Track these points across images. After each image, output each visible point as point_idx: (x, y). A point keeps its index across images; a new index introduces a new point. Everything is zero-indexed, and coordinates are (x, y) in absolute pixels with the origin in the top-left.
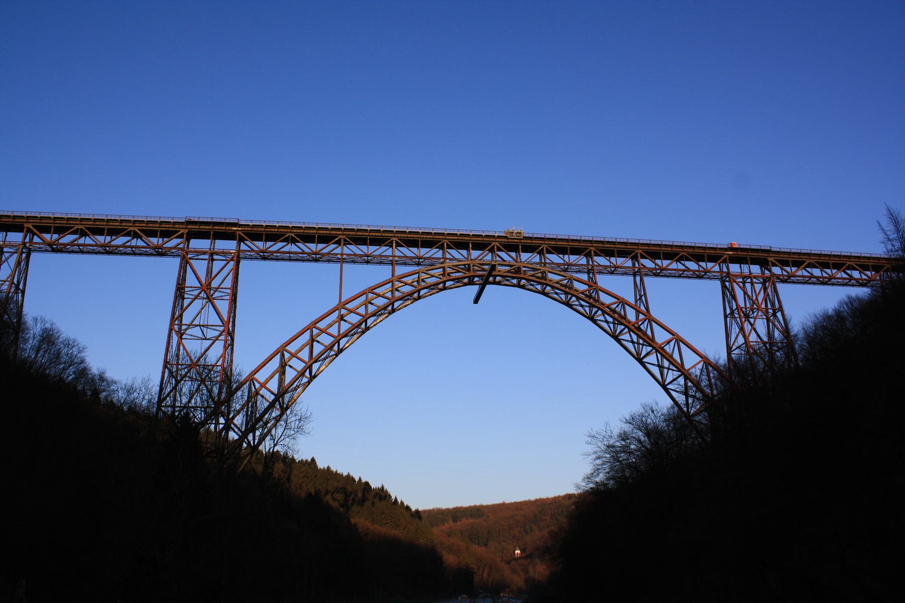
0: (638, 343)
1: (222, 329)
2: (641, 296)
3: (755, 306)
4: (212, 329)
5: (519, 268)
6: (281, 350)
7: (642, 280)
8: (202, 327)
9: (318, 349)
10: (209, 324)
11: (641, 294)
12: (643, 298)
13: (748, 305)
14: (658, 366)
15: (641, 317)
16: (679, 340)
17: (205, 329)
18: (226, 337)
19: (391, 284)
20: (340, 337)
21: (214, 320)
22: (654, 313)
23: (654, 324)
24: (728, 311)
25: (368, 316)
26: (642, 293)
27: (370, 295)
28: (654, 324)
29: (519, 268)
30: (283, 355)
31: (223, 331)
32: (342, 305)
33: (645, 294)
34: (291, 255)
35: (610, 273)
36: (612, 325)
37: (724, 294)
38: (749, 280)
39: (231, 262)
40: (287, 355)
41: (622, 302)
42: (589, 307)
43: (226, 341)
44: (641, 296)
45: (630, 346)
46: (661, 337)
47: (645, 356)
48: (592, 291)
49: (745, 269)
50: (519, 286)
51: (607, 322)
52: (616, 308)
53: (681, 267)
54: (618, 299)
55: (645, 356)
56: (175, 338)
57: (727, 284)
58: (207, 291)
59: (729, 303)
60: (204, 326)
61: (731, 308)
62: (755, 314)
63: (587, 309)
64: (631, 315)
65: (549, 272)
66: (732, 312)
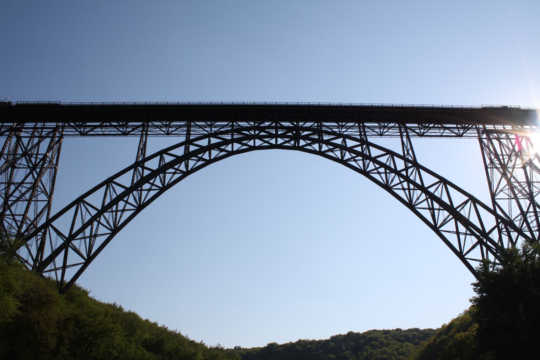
0: (409, 189)
2: (408, 151)
7: (408, 137)
11: (408, 147)
12: (410, 152)
14: (429, 209)
15: (410, 165)
22: (420, 161)
24: (488, 162)
26: (409, 147)
28: (421, 171)
33: (412, 148)
34: (101, 133)
35: (380, 135)
36: (383, 176)
37: (482, 148)
39: (47, 138)
41: (392, 154)
44: (408, 151)
45: (401, 193)
46: (428, 180)
52: (386, 163)
64: (400, 164)
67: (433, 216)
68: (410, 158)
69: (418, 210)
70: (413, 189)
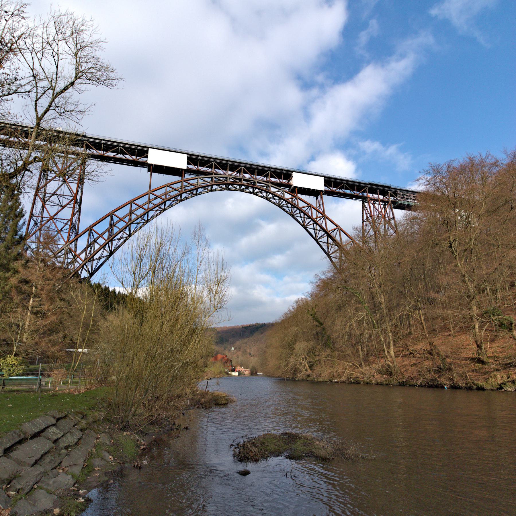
1: (71, 198)
2: (320, 205)
3: (380, 215)
4: (66, 198)
5: (255, 182)
6: (111, 214)
8: (59, 197)
9: (134, 217)
10: (64, 194)
12: (321, 206)
13: (375, 214)
15: (320, 215)
16: (341, 230)
17: (61, 199)
18: (74, 206)
19: (181, 183)
20: (149, 210)
21: (67, 192)
22: (327, 214)
23: (327, 220)
24: (365, 218)
25: (166, 200)
26: (321, 203)
27: (169, 189)
29: (255, 182)
30: (112, 218)
31: (72, 200)
32: (151, 192)
33: (323, 204)
36: (303, 219)
38: (377, 203)
40: (115, 219)
42: (292, 208)
43: (74, 208)
44: (320, 205)
47: (320, 238)
48: (294, 199)
49: (376, 196)
50: (253, 193)
51: (301, 217)
53: (341, 191)
54: (308, 205)
55: (320, 238)
56: (39, 204)
57: (366, 204)
58: (63, 175)
59: (366, 214)
60: (60, 195)
61: (367, 217)
62: (380, 221)
63: (290, 209)
65: (271, 186)
66: (367, 218)
67: (328, 249)
68: (320, 210)
69: (320, 242)
70: (319, 230)
